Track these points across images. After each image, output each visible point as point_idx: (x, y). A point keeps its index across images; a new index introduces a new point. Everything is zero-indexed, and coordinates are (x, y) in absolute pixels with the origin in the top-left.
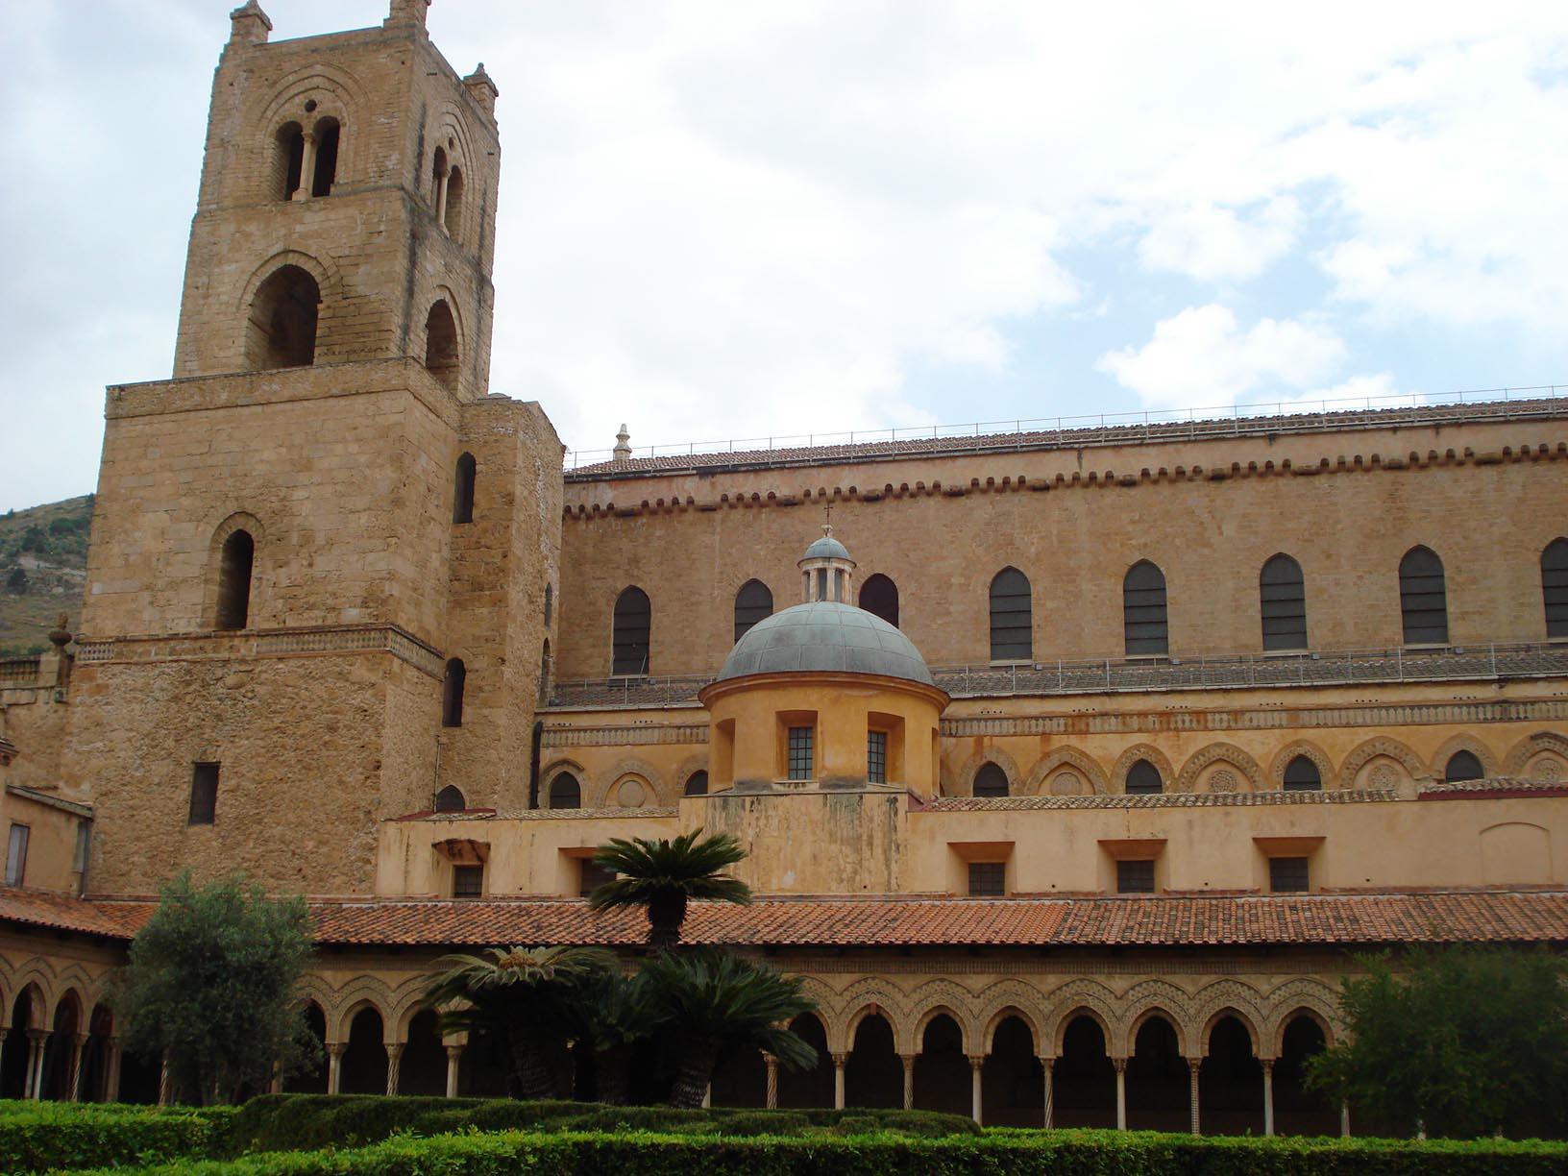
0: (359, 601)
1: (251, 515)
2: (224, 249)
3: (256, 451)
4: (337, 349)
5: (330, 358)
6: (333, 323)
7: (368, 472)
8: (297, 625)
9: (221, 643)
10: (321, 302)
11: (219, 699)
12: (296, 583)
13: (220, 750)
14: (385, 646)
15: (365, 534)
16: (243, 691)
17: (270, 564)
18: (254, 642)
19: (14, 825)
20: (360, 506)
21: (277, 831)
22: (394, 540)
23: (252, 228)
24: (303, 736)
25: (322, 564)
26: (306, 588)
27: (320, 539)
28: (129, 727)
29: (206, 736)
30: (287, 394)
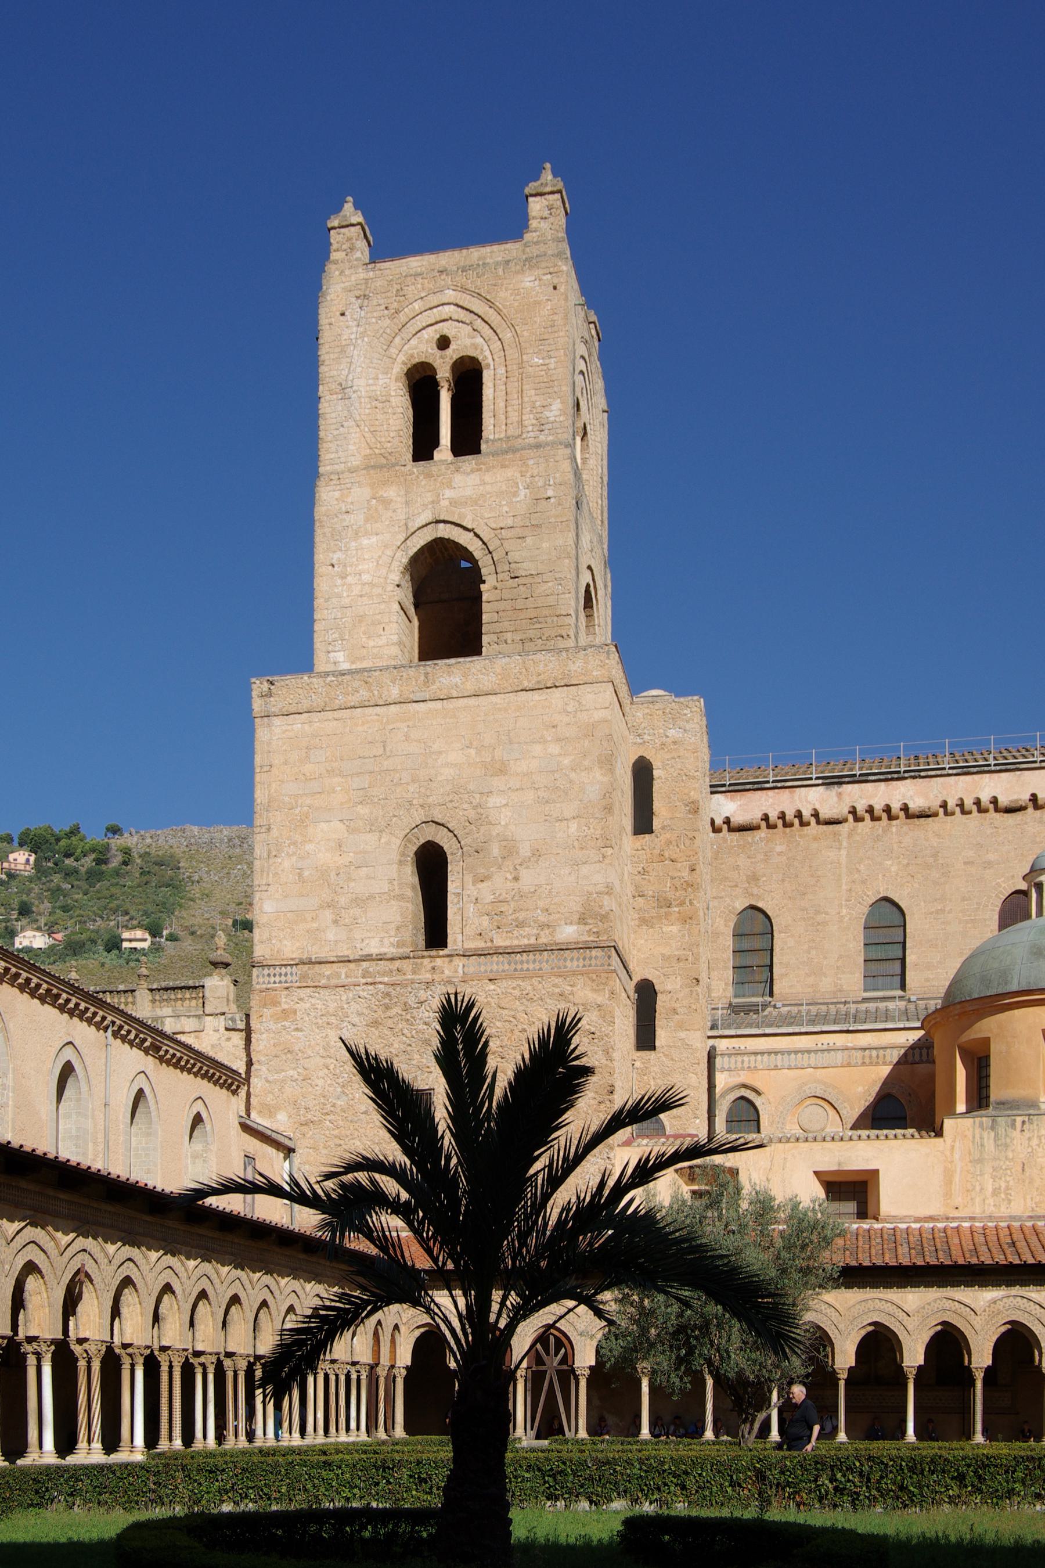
0: (576, 917)
1: (443, 825)
2: (357, 519)
3: (440, 753)
4: (509, 636)
5: (503, 647)
6: (501, 605)
7: (573, 775)
8: (507, 943)
9: (422, 964)
10: (484, 582)
11: (426, 1024)
12: (501, 898)
14: (609, 965)
15: (576, 844)
17: (469, 878)
18: (459, 962)
19: (246, 1156)
20: (567, 814)
22: (609, 851)
23: (391, 492)
25: (529, 878)
26: (512, 904)
27: (525, 850)
28: (325, 1054)
29: (414, 1062)
30: (470, 687)
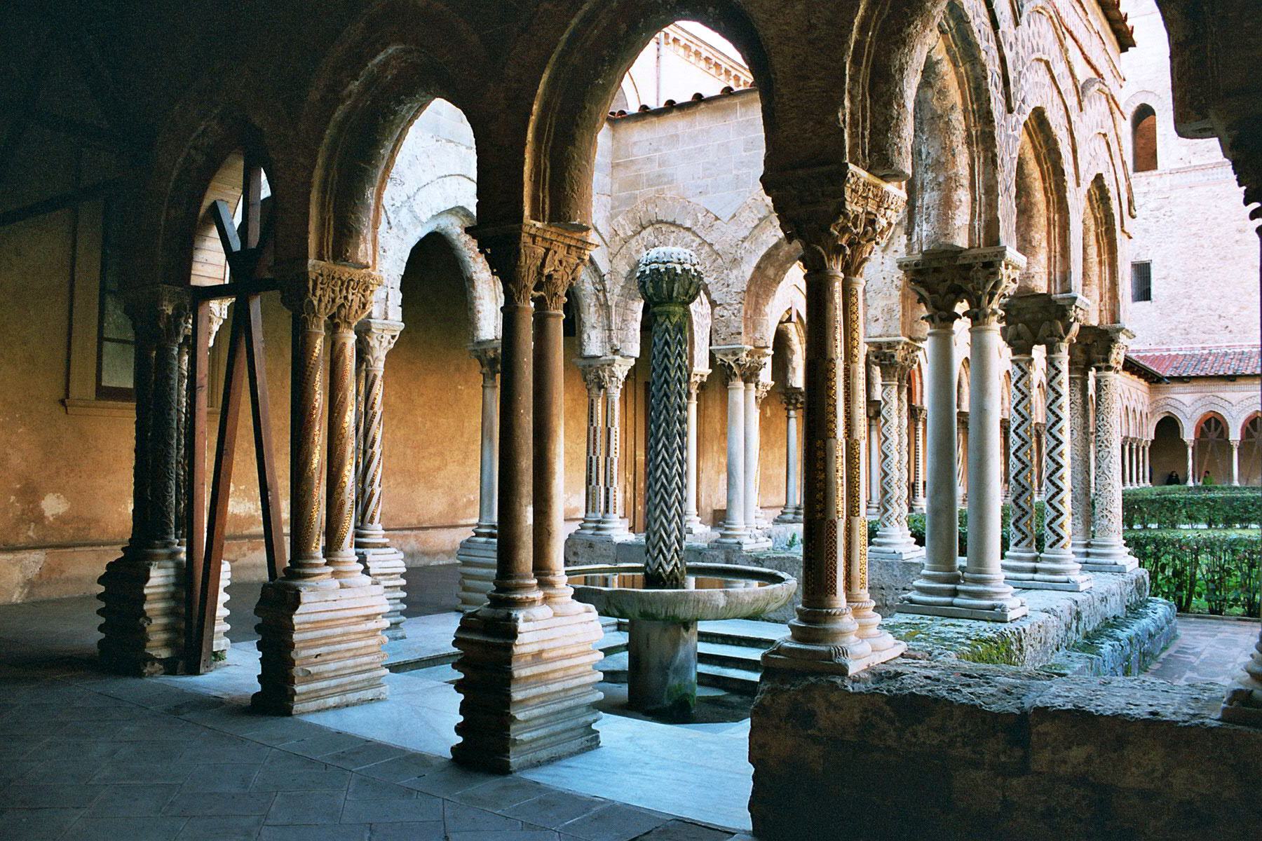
1: (1152, 92)
11: (1144, 219)
13: (1150, 252)
16: (1163, 211)
18: (1168, 178)
21: (1204, 302)
24: (1217, 238)
